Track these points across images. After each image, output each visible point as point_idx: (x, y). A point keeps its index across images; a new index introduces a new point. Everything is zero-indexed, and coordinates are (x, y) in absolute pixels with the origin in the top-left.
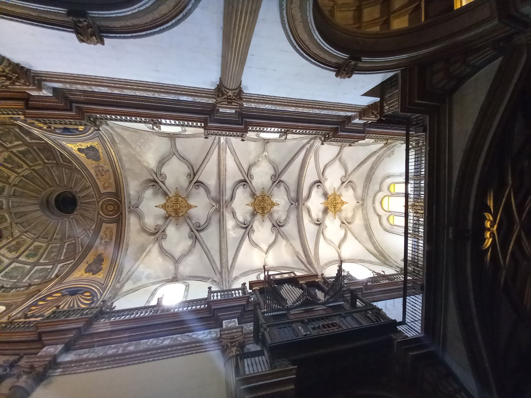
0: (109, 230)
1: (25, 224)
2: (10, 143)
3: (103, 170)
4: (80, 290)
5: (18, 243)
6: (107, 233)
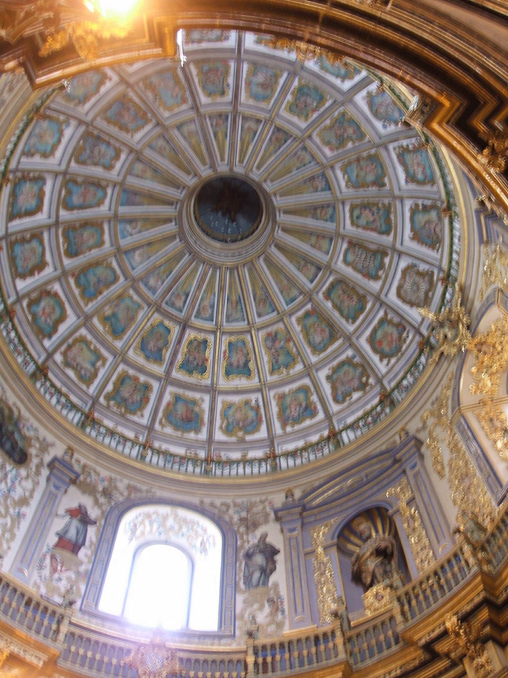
2: (247, 403)
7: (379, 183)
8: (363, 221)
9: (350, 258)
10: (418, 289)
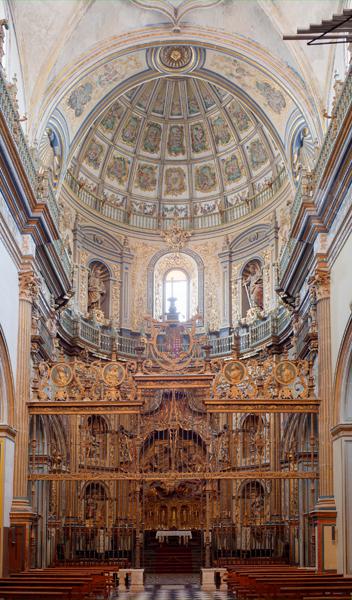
0: (217, 61)
1: (208, 101)
3: (106, 75)
4: (299, 136)
5: (236, 115)
6: (222, 64)
7: (216, 140)
8: (195, 132)
9: (174, 130)
10: (175, 183)
